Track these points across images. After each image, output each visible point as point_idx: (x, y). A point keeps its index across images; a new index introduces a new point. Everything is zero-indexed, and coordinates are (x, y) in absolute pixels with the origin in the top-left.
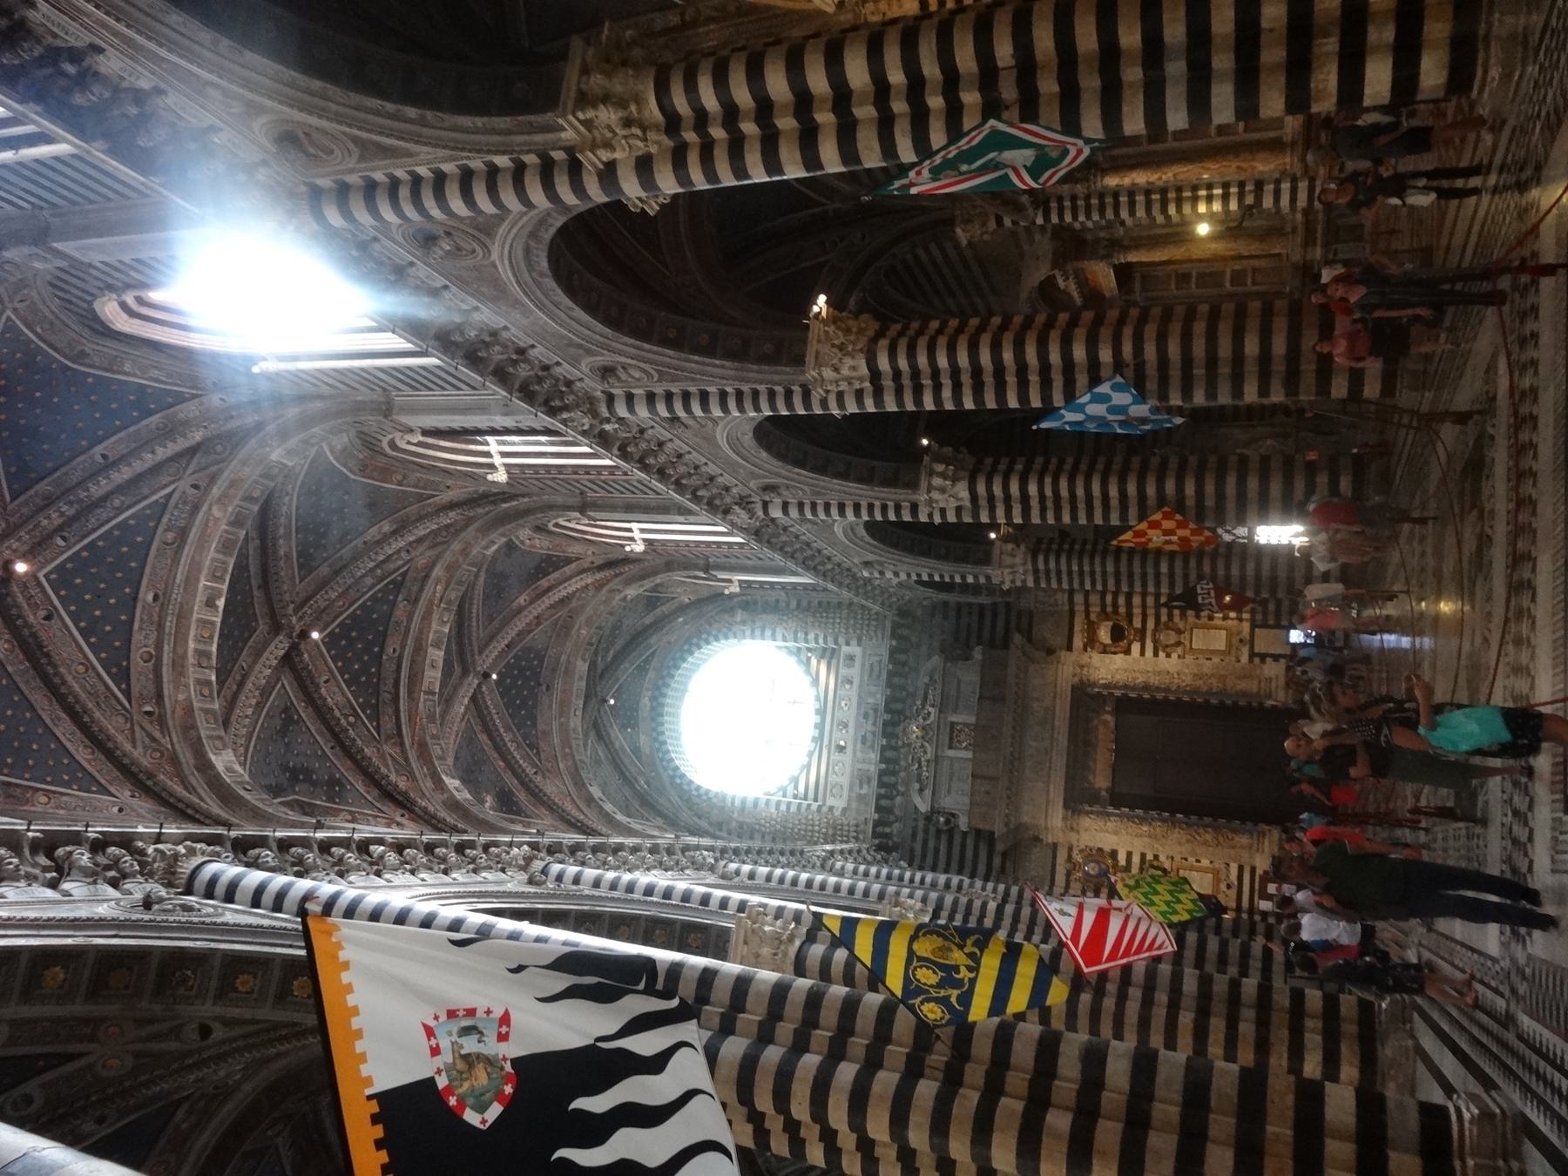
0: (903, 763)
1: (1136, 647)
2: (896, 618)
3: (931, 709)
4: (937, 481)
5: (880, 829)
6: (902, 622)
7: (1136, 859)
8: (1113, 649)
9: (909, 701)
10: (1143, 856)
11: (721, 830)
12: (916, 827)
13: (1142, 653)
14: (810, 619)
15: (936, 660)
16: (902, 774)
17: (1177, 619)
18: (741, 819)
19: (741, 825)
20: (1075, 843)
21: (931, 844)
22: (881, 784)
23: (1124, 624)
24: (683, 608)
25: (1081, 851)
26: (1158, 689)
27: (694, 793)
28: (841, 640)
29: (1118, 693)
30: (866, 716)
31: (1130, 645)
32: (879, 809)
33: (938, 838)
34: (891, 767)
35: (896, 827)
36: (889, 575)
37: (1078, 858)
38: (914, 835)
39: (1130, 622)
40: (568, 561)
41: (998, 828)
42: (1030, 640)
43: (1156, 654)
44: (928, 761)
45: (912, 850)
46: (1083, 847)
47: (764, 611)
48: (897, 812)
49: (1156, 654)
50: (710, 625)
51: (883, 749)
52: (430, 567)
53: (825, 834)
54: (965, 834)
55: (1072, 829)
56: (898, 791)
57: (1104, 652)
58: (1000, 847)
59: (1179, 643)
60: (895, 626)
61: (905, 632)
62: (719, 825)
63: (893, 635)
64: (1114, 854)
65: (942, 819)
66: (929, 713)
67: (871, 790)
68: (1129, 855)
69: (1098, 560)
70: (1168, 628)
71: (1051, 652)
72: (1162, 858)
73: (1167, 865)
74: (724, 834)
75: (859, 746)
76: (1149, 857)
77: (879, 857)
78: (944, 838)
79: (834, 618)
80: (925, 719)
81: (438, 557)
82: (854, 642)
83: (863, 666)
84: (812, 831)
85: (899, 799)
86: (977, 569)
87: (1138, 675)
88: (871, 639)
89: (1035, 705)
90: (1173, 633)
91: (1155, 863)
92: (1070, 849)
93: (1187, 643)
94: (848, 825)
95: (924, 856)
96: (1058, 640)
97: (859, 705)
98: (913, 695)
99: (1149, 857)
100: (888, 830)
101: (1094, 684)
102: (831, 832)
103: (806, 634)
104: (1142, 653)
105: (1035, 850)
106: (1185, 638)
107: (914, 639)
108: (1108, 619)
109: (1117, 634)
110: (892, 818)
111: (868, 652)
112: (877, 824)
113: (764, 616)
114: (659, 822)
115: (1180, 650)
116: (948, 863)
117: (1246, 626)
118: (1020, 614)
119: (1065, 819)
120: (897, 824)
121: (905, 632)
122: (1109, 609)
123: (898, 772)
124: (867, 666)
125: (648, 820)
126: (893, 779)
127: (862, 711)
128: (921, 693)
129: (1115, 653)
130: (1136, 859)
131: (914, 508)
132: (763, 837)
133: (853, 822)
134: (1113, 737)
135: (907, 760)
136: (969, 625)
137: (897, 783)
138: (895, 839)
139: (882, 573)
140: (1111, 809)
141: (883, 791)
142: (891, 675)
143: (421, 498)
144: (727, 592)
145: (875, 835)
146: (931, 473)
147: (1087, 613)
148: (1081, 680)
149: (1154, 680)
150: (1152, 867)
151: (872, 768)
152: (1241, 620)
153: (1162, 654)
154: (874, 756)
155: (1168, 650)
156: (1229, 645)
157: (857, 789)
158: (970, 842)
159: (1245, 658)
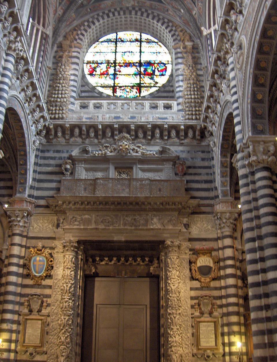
0: (103, 141)
1: (196, 284)
2: (198, 128)
5: (59, 129)
6: (197, 133)
7: (47, 291)
8: (193, 268)
9: (144, 141)
10: (49, 296)
11: (58, 47)
12: (63, 152)
14: (192, 82)
16: (96, 141)
17: (220, 310)
18: (64, 56)
19: (61, 57)
20: (56, 250)
21: (52, 162)
23: (212, 275)
24: (189, 11)
25: (51, 256)
26: (167, 300)
27: (79, 32)
28: (180, 100)
31: (197, 280)
32: (73, 127)
33: (57, 166)
34: (100, 133)
35: (62, 140)
36: (232, 75)
38: (58, 151)
39: (214, 279)
44: (106, 153)
45: (48, 151)
46: (55, 256)
48: (72, 140)
49: (192, 298)
50: (181, 31)
53: (57, 101)
55: (64, 247)
56: (85, 139)
57: (190, 263)
60: (192, 127)
61: (190, 134)
62: (60, 46)
63: (188, 127)
64: (49, 276)
65: (68, 167)
66: (137, 152)
68: (50, 287)
69: (270, 219)
70: (213, 305)
72: (49, 309)
73: (44, 311)
74: (55, 48)
76: (49, 301)
77: (40, 127)
78: (57, 169)
79: (194, 94)
80: (133, 150)
84: (58, 94)
85: (79, 140)
87: (176, 285)
88: (182, 117)
90: (209, 308)
91: (45, 304)
93: (202, 319)
94: (63, 113)
95: (45, 158)
99: (49, 301)
100: (60, 134)
102: (58, 104)
103: (182, 81)
104: (191, 289)
105: (50, 226)
106: (206, 318)
107: (186, 141)
108: (215, 263)
109: (205, 271)
110: (67, 137)
111: (174, 116)
112: (62, 127)
113: (190, 57)
114: (60, 12)
116: (40, 173)
118: (212, 206)
119: (70, 242)
120: (64, 140)
121: (190, 134)
122: (222, 264)
123: (97, 138)
124: (165, 116)
125: (60, 4)
126: (92, 135)
127: (135, 115)
129: (191, 270)
130: (47, 291)
132: (54, 69)
133: (64, 116)
135: (105, 143)
136: (200, 174)
137: (90, 138)
138: (55, 140)
139: (233, 69)
141: (84, 128)
142: (160, 127)
144: (202, 28)
145: (56, 127)
148: (169, 246)
149: (173, 296)
150: (42, 302)
151: (100, 119)
155: (197, 306)
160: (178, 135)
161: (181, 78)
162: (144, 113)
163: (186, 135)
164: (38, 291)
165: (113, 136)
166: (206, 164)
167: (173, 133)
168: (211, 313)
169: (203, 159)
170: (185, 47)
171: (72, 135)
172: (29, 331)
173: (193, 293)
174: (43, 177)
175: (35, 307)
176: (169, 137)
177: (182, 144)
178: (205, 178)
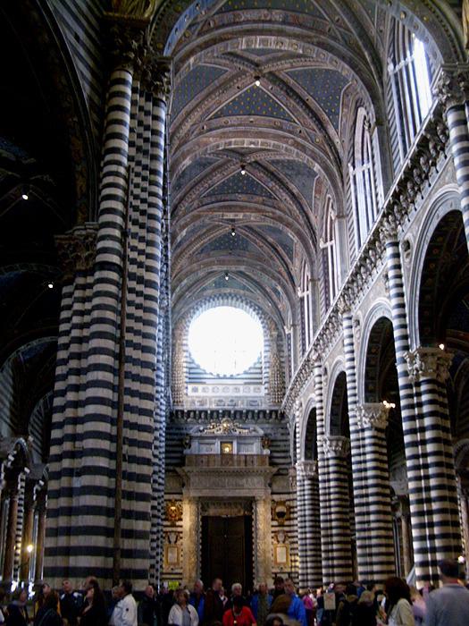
1: (275, 523)
3: (238, 432)
4: (334, 443)
7: (179, 529)
13: (273, 526)
15: (261, 432)
22: (201, 412)
26: (257, 535)
28: (266, 385)
29: (253, 517)
30: (232, 401)
32: (189, 412)
37: (178, 503)
39: (287, 520)
40: (291, 259)
41: (186, 469)
42: (275, 475)
43: (272, 532)
47: (278, 346)
49: (272, 532)
51: (217, 412)
52: (279, 209)
54: (182, 452)
58: (178, 469)
59: (278, 542)
61: (274, 416)
64: (181, 520)
65: (187, 441)
67: (197, 406)
71: (270, 485)
73: (178, 543)
75: (217, 399)
78: (178, 443)
81: (284, 212)
82: (267, 391)
83: (257, 397)
86: (303, 454)
89: (244, 480)
92: (181, 500)
96: (275, 488)
97: (236, 397)
98: (244, 422)
99: (181, 535)
101: (256, 506)
104: (273, 526)
108: (287, 510)
112: (182, 412)
113: (275, 345)
115: (275, 542)
117: (289, 570)
118: (287, 469)
121: (274, 416)
124: (255, 399)
128: (245, 426)
131: (322, 433)
134: (233, 516)
140: (200, 517)
141: (197, 412)
143: (310, 205)
145: (177, 411)
146: (338, 440)
147: (289, 500)
152: (291, 567)
153: (273, 534)
154: (214, 407)
156: (280, 564)
157: (197, 399)
158: (179, 455)
159: (274, 571)
160: (264, 417)
161: (268, 365)
162: (240, 397)
163: (271, 417)
164: (174, 529)
165: (218, 417)
166: (284, 438)
167: (261, 416)
168: (284, 542)
169: (282, 434)
170: (271, 336)
171: (189, 417)
172: (170, 555)
173: (274, 529)
174: (171, 449)
175: (173, 540)
176: (259, 417)
177: (268, 423)
178: (284, 448)
